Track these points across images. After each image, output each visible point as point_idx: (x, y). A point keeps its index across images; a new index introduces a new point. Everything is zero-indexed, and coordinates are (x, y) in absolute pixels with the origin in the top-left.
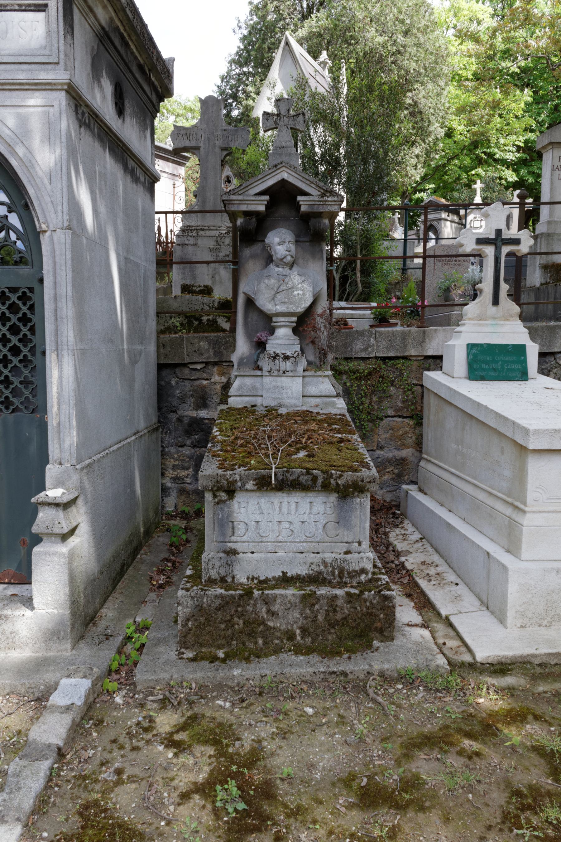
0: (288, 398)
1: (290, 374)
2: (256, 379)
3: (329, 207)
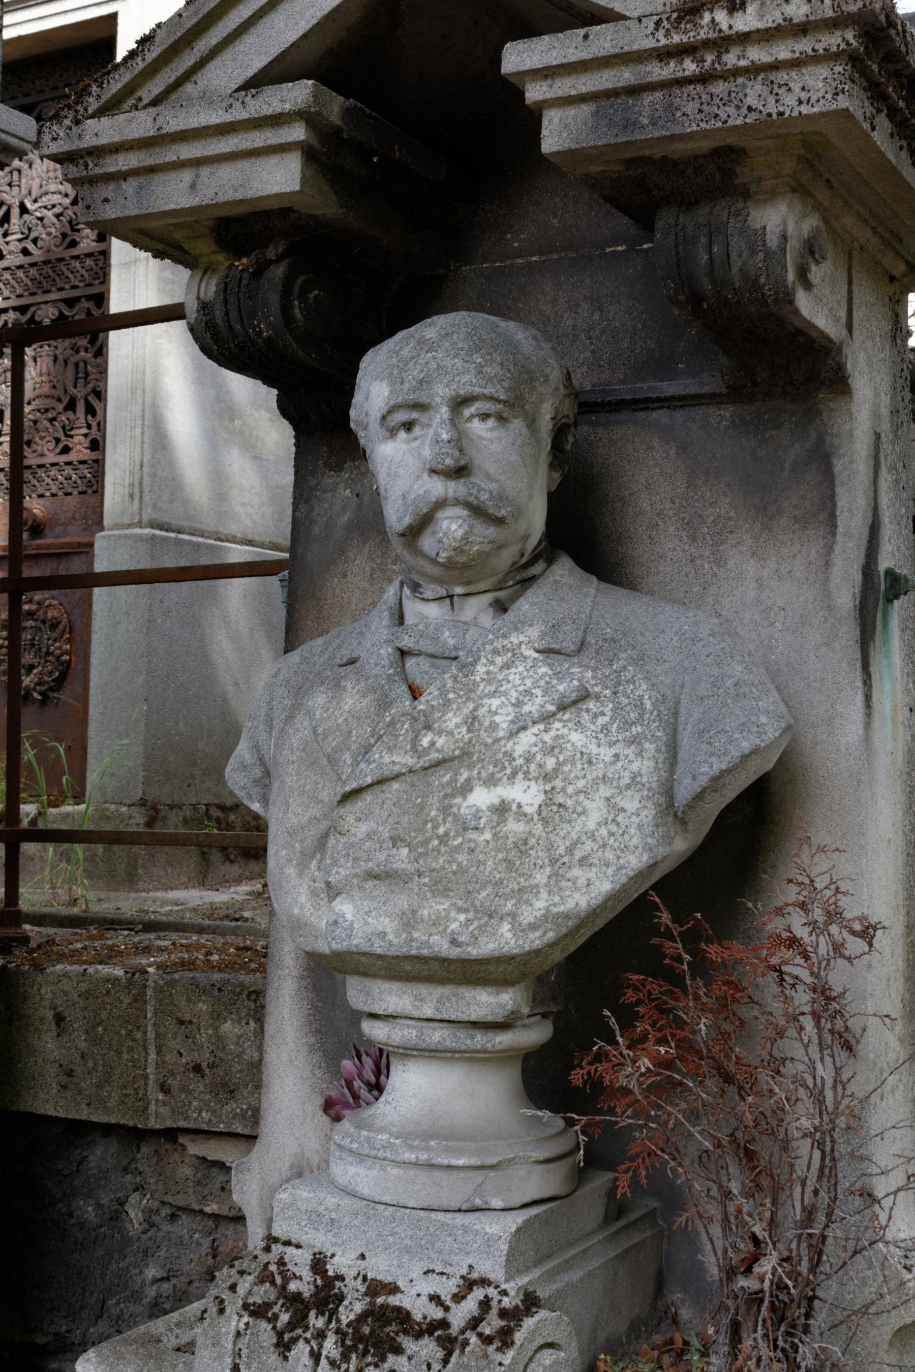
3: (754, 92)
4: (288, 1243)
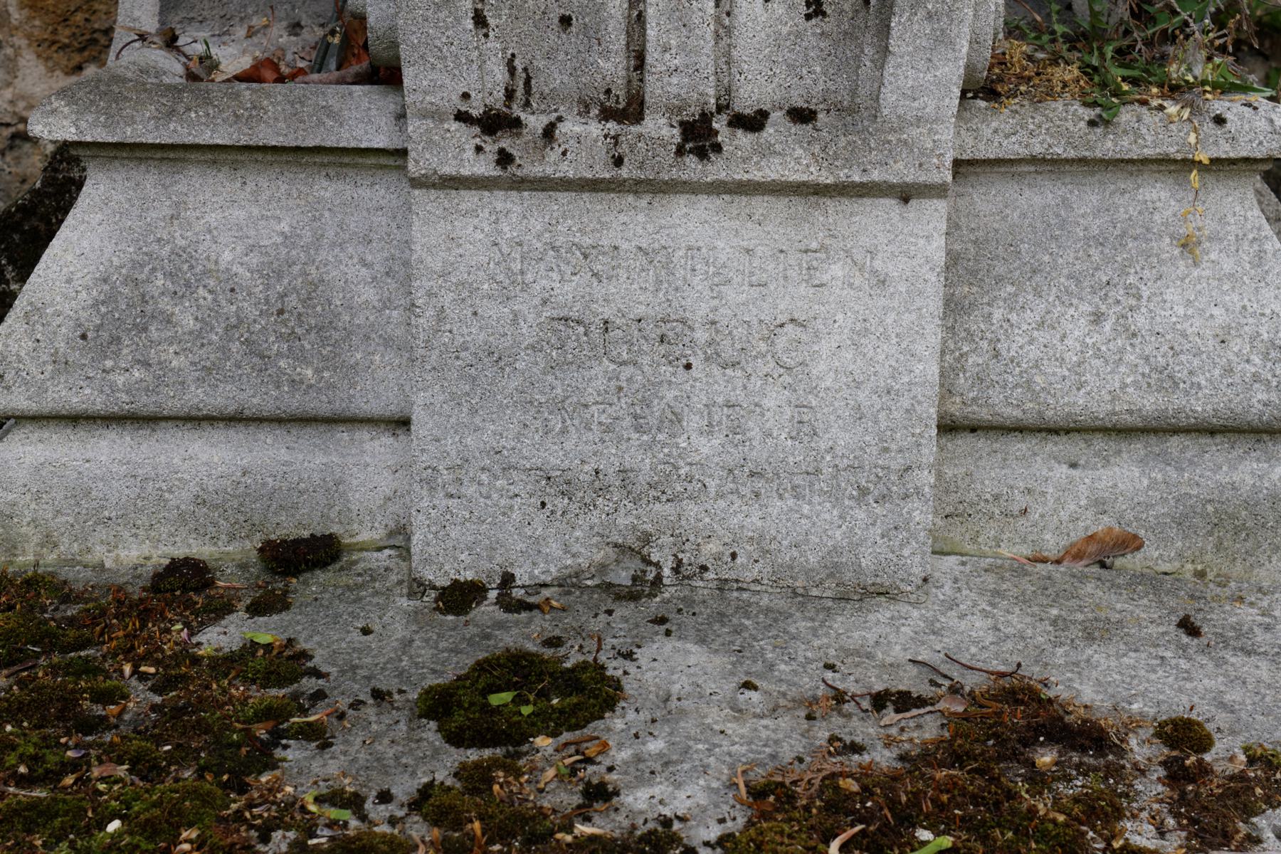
0: (754, 477)
1: (787, 156)
2: (326, 189)
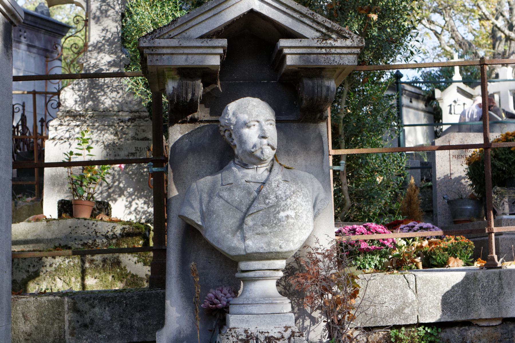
4: (234, 328)
